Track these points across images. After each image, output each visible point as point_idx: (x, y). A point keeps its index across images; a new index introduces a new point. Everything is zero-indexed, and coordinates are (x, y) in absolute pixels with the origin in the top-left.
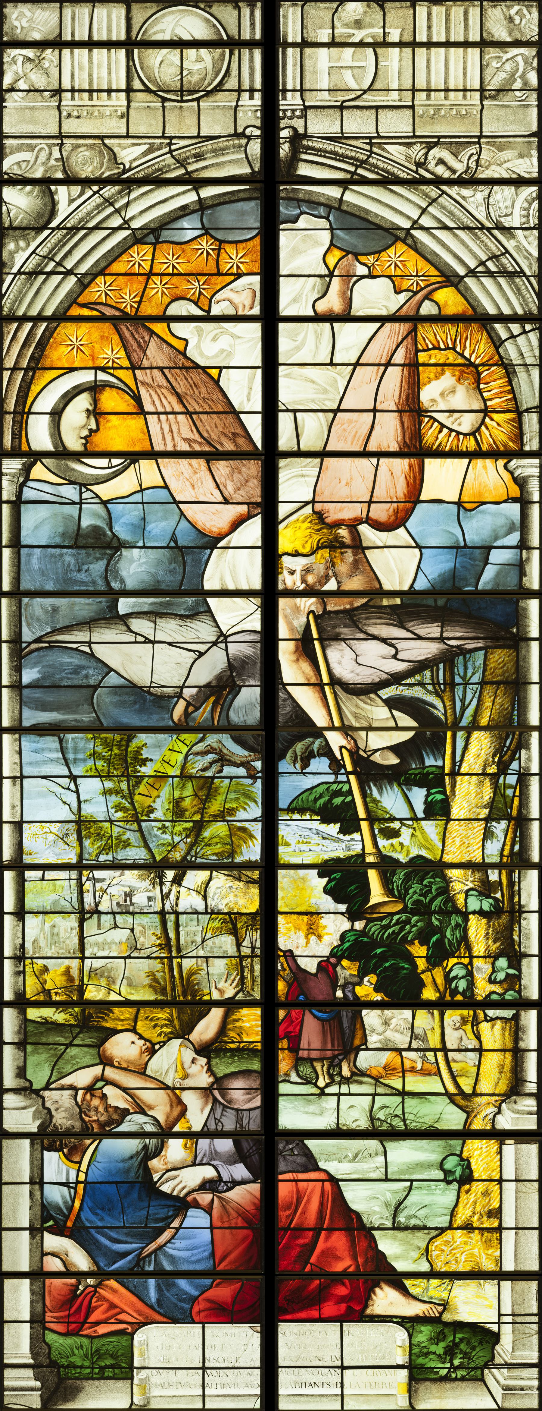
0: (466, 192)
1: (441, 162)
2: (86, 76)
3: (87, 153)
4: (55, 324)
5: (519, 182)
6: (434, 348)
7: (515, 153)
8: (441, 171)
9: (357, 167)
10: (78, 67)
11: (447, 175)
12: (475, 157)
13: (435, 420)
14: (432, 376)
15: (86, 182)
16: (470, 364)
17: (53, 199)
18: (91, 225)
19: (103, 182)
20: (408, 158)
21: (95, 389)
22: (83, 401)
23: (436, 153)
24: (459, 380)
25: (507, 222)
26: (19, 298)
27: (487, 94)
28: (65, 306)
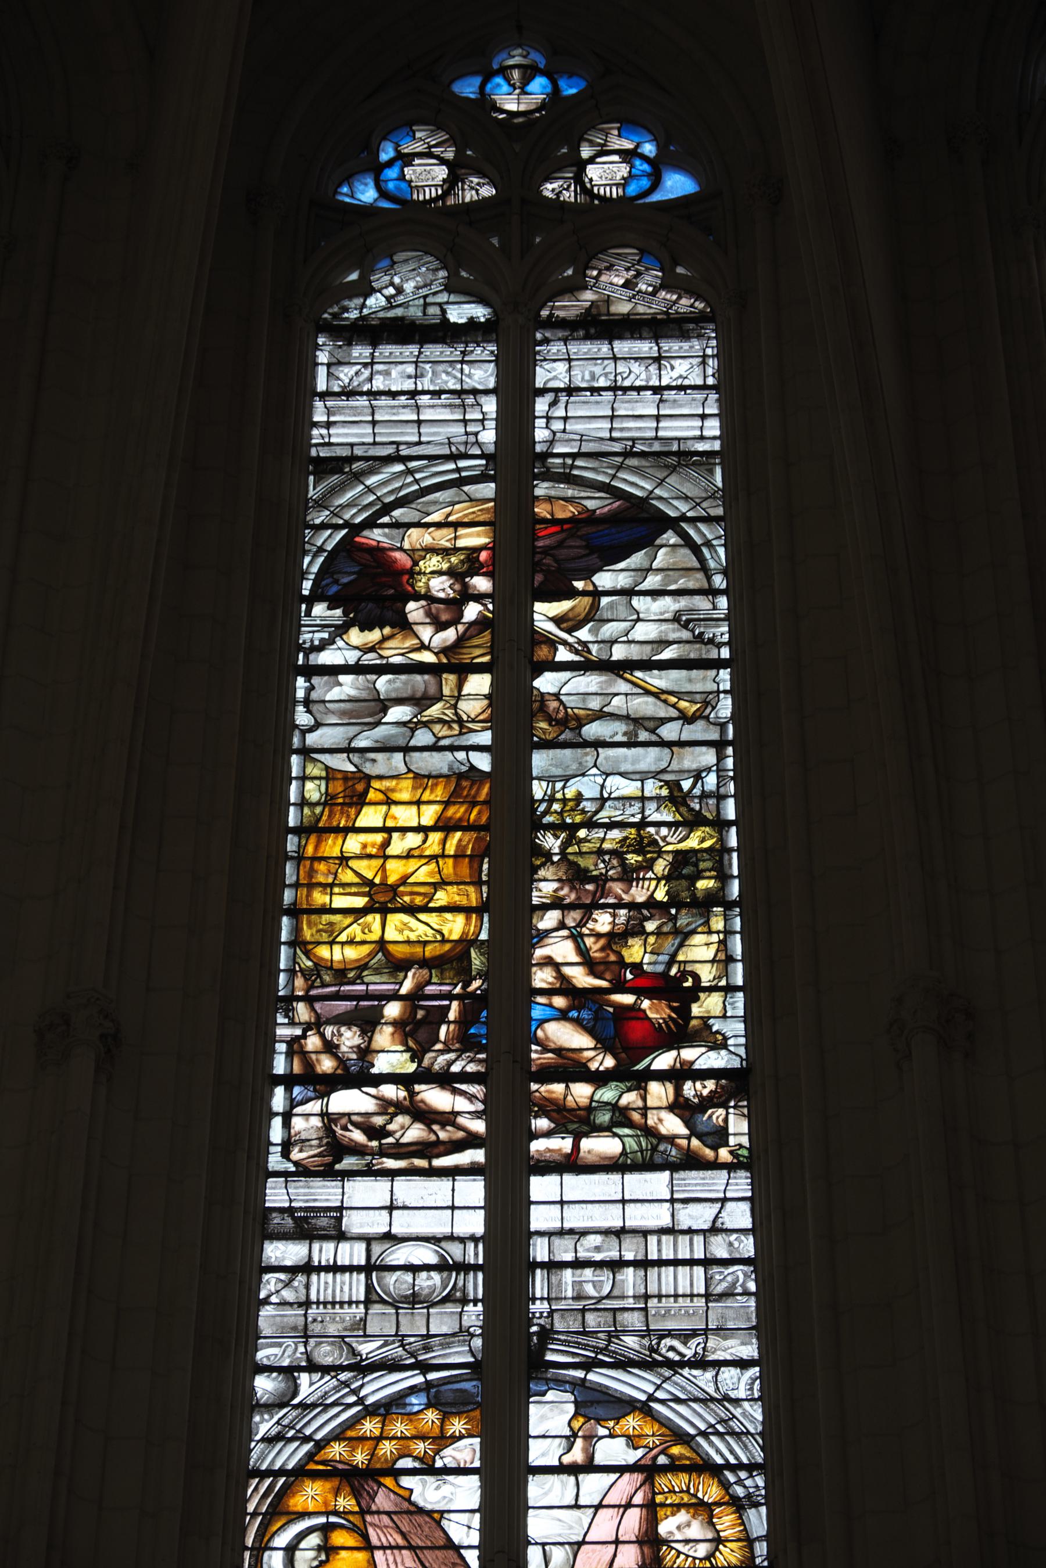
0: (695, 1372)
1: (672, 1348)
2: (330, 1291)
3: (328, 1348)
4: (292, 1479)
5: (742, 1364)
6: (670, 1491)
7: (738, 1342)
8: (671, 1355)
9: (597, 1353)
10: (321, 1285)
11: (677, 1358)
12: (702, 1345)
13: (673, 1548)
14: (668, 1513)
15: (325, 1370)
16: (701, 1503)
17: (296, 1383)
18: (329, 1401)
19: (342, 1368)
20: (642, 1346)
21: (326, 1529)
22: (314, 1540)
23: (668, 1342)
24: (693, 1517)
25: (733, 1395)
26: (262, 1457)
27: (712, 1298)
28: (304, 1462)
